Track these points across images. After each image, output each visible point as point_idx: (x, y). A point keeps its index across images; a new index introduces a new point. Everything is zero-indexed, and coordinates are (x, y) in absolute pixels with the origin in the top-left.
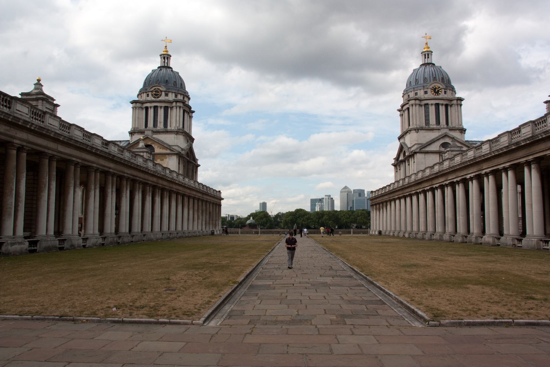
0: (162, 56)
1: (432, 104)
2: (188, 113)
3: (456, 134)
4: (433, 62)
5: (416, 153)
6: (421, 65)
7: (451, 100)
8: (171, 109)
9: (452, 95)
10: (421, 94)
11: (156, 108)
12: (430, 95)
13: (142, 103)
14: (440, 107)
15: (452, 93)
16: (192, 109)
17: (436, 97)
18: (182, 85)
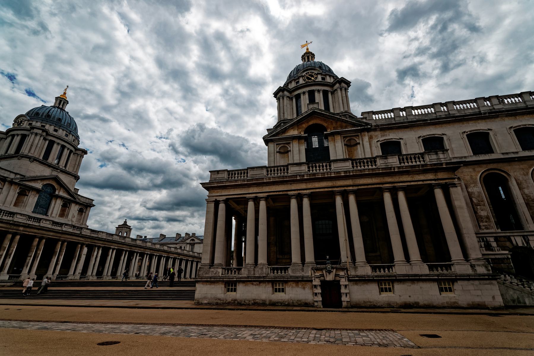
7: (332, 85)
11: (13, 136)
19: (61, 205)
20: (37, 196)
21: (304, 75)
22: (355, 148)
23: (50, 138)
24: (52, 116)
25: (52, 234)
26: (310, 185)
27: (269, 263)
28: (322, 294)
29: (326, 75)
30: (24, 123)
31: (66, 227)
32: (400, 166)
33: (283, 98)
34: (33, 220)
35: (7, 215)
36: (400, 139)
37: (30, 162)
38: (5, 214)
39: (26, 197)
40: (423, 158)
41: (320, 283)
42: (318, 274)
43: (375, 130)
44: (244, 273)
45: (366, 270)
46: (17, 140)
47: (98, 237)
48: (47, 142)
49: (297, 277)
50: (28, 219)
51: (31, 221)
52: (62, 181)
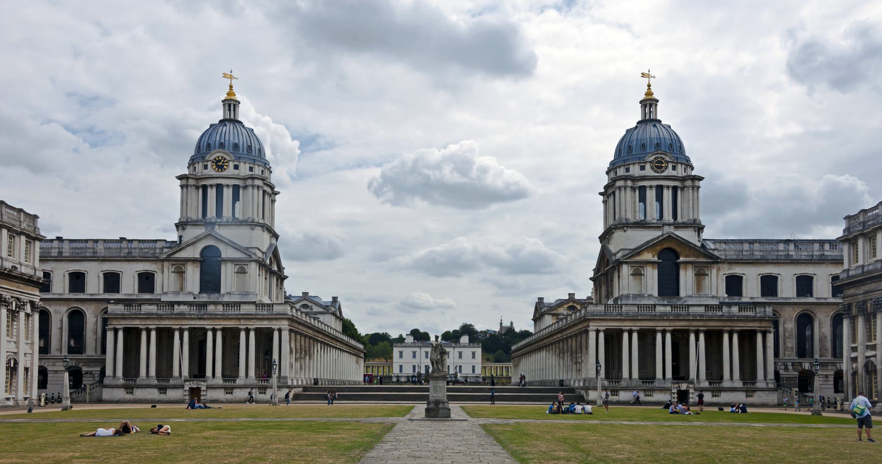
0: (226, 102)
1: (651, 187)
2: (270, 195)
3: (688, 235)
4: (658, 118)
5: (622, 263)
6: (638, 123)
7: (683, 179)
8: (243, 190)
9: (685, 172)
10: (635, 170)
11: (219, 188)
12: (649, 171)
13: (197, 179)
14: (665, 191)
15: (685, 168)
16: (276, 190)
17: (656, 176)
18: (261, 151)
21: (653, 160)
22: (703, 277)
23: (266, 188)
24: (253, 145)
26: (672, 324)
27: (640, 378)
28: (677, 398)
29: (677, 163)
32: (738, 314)
33: (625, 189)
36: (743, 274)
40: (755, 308)
41: (676, 391)
42: (676, 386)
43: (723, 263)
44: (623, 384)
45: (706, 384)
49: (662, 387)
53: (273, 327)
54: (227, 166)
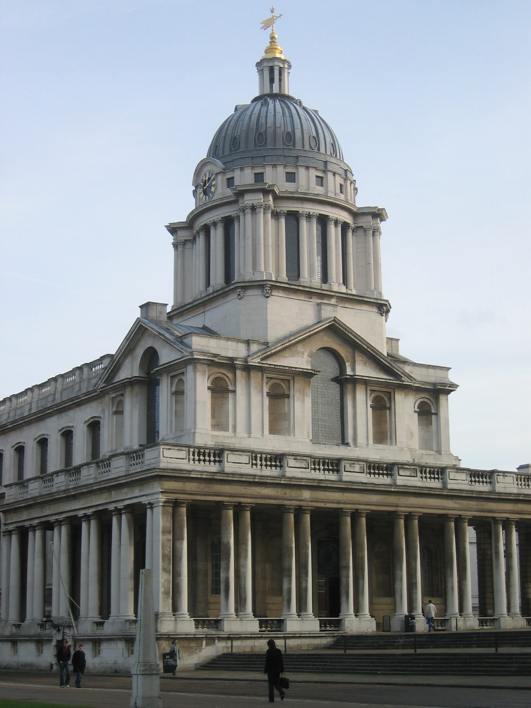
19: (371, 407)
20: (309, 392)
24: (270, 131)
25: (374, 498)
30: (217, 183)
31: (402, 472)
34: (324, 465)
35: (269, 463)
37: (265, 299)
38: (264, 463)
39: (286, 400)
46: (217, 235)
47: (493, 492)
48: (283, 221)
50: (313, 467)
51: (319, 469)
52: (352, 332)
53: (144, 500)
54: (214, 186)
